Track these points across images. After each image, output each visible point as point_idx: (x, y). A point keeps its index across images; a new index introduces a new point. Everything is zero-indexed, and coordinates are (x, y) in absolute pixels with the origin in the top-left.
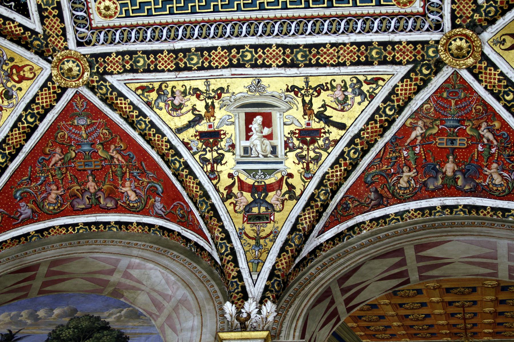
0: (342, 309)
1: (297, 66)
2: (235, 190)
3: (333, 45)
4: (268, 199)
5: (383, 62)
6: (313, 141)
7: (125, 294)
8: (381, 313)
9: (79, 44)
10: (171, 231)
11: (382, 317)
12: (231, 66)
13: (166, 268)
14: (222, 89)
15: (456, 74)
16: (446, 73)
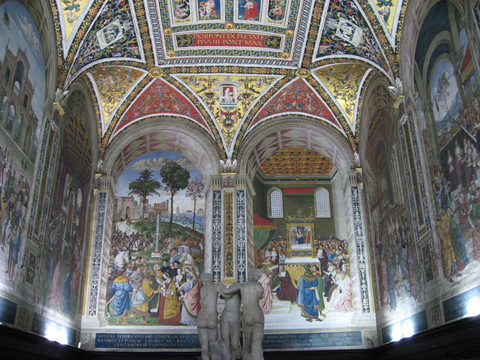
0: (258, 161)
1: (244, 73)
2: (220, 114)
3: (258, 68)
4: (232, 118)
5: (275, 74)
6: (248, 97)
7: (183, 151)
8: (270, 162)
9: (159, 65)
10: (193, 122)
11: (271, 164)
12: (219, 72)
13: (194, 139)
14: (215, 79)
15: (300, 79)
16: (297, 78)
